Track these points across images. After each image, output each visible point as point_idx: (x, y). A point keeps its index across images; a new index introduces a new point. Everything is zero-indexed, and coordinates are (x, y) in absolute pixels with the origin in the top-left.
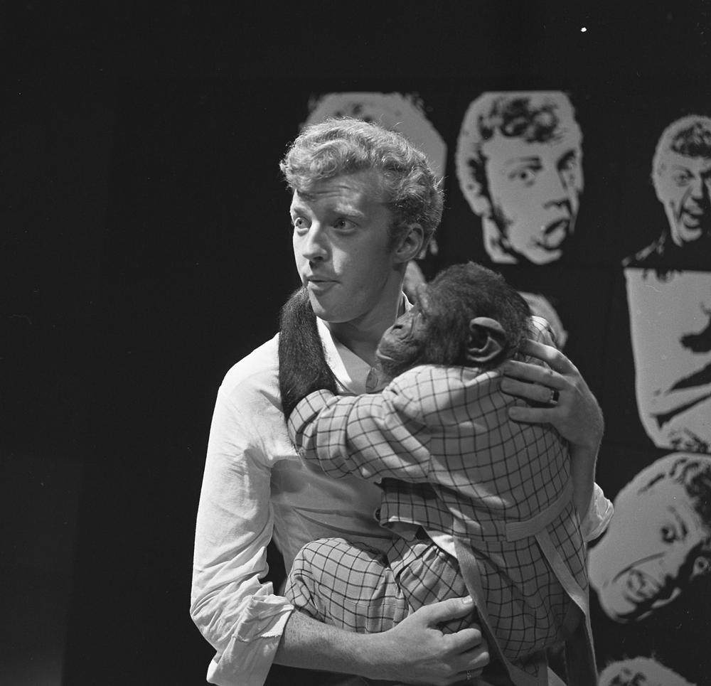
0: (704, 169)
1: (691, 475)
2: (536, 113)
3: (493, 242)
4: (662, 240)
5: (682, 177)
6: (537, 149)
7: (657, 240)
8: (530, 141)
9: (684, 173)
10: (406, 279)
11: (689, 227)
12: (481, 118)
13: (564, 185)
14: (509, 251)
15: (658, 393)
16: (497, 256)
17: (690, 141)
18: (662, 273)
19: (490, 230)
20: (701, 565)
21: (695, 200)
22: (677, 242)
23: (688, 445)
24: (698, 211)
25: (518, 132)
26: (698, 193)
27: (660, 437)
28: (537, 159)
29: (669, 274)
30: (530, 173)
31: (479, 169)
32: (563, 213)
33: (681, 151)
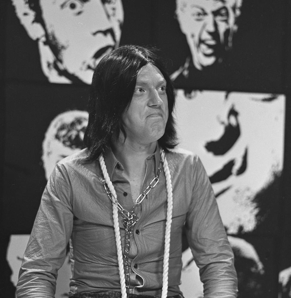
3: (49, 65)
4: (187, 65)
5: (199, 14)
7: (183, 65)
9: (200, 11)
22: (198, 67)
24: (212, 43)
26: (212, 29)
29: (193, 94)
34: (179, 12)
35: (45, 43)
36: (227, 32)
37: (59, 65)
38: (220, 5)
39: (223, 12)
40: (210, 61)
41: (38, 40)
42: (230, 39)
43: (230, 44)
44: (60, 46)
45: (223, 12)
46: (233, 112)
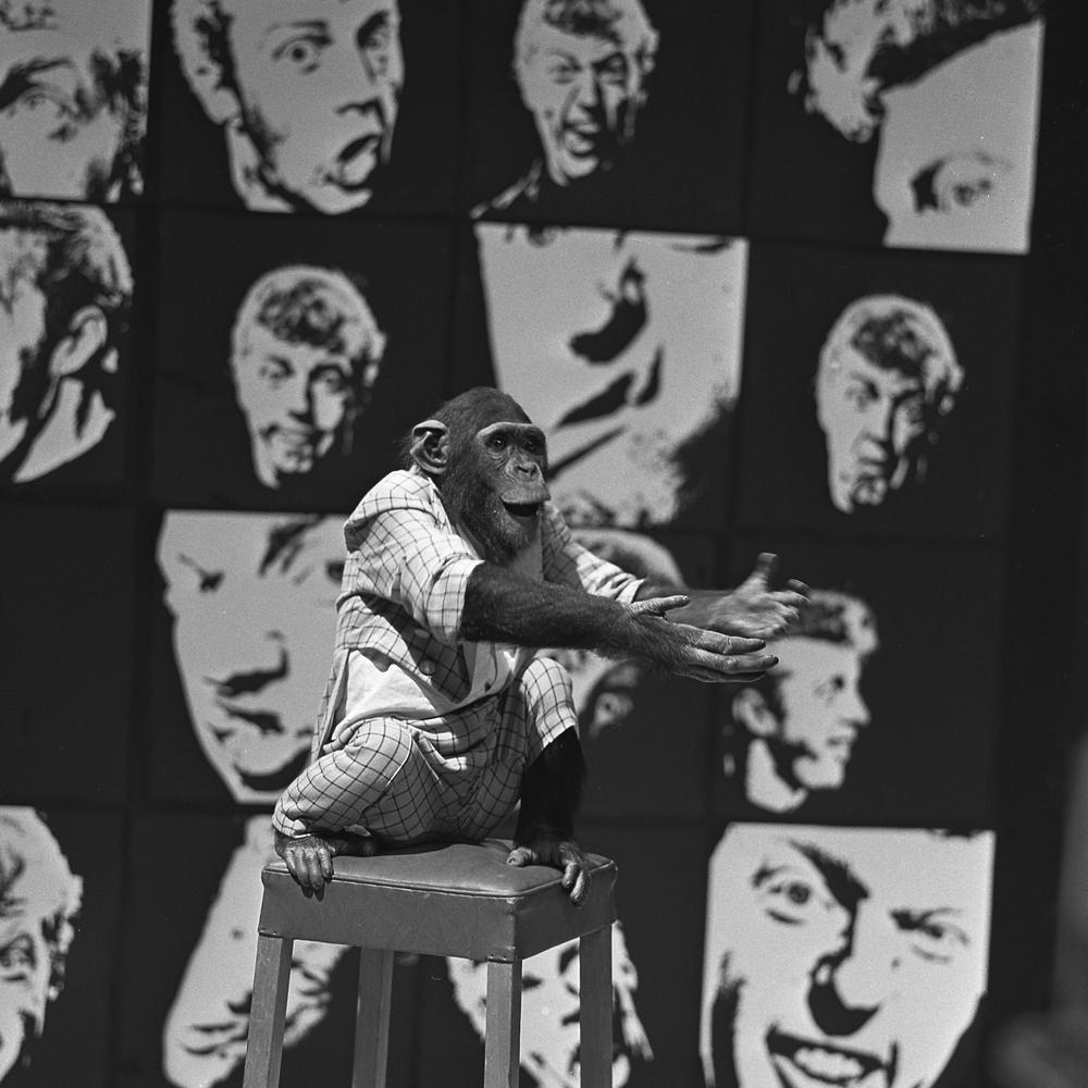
0: (598, 56)
3: (247, 174)
4: (535, 175)
5: (564, 69)
7: (525, 173)
9: (563, 61)
10: (86, 241)
13: (371, 74)
14: (277, 190)
16: (258, 199)
17: (573, 8)
19: (242, 152)
20: (608, 707)
22: (559, 179)
23: (586, 516)
24: (590, 128)
26: (588, 98)
28: (321, 25)
29: (547, 234)
30: (309, 48)
32: (370, 124)
33: (559, 22)
34: (521, 64)
35: (242, 129)
36: (624, 106)
38: (608, 48)
39: (616, 63)
40: (585, 167)
41: (226, 123)
42: (630, 120)
43: (629, 132)
44: (269, 136)
45: (616, 63)
46: (632, 274)
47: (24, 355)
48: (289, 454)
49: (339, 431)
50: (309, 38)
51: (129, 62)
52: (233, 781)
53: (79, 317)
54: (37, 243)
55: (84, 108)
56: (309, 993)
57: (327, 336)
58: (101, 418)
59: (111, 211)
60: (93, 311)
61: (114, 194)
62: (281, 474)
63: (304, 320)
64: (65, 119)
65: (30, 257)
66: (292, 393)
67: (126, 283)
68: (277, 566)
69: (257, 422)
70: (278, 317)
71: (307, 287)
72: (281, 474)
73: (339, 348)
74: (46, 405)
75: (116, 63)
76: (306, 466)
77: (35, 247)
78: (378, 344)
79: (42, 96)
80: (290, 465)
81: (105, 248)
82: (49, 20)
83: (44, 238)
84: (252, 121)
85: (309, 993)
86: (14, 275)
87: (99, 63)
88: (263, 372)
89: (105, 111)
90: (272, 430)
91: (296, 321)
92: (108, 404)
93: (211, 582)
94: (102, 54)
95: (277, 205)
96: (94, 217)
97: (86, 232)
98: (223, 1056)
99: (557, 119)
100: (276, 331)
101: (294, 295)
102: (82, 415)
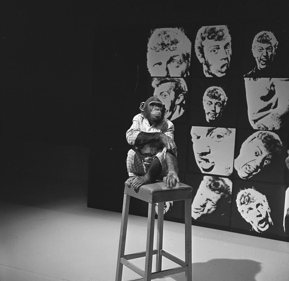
0: (267, 47)
1: (263, 137)
2: (218, 32)
3: (206, 71)
4: (255, 69)
5: (260, 50)
6: (218, 43)
8: (216, 40)
11: (262, 65)
12: (202, 34)
13: (226, 53)
14: (210, 74)
15: (254, 114)
16: (207, 75)
18: (255, 79)
19: (205, 68)
20: (266, 162)
21: (264, 56)
22: (260, 69)
24: (266, 60)
25: (212, 38)
26: (265, 54)
27: (255, 126)
28: (218, 46)
29: (257, 79)
30: (216, 50)
31: (201, 49)
32: (226, 62)
33: (260, 42)
34: (253, 49)
35: (205, 64)
36: (272, 55)
37: (209, 71)
38: (269, 45)
40: (264, 66)
41: (203, 63)
46: (273, 85)
47: (172, 101)
48: (211, 117)
49: (220, 113)
50: (216, 48)
51: (188, 54)
52: (202, 170)
53: (180, 95)
54: (174, 84)
55: (181, 63)
56: (213, 205)
57: (218, 98)
58: (182, 111)
59: (184, 78)
60: (182, 94)
61: (185, 76)
62: (210, 120)
63: (214, 95)
64: (178, 64)
65: (173, 86)
66: (212, 107)
67: (187, 90)
68: (209, 135)
69: (206, 112)
70: (210, 95)
71: (215, 89)
72: (210, 120)
73: (220, 100)
74: (175, 109)
75: (186, 55)
76: (214, 119)
77: (173, 84)
78: (227, 99)
79: (174, 61)
80: (211, 119)
81: (183, 84)
82: (176, 49)
83: (174, 83)
84: (207, 62)
85: (213, 205)
86: (170, 89)
87: (183, 55)
88: (207, 104)
89: (184, 62)
90: (209, 113)
91: (213, 95)
92: (183, 109)
93: (198, 137)
94: (184, 54)
95: (210, 76)
96: (182, 79)
97: (181, 82)
98: (199, 213)
99: (259, 59)
100: (210, 97)
101: (213, 91)
102: (180, 111)
